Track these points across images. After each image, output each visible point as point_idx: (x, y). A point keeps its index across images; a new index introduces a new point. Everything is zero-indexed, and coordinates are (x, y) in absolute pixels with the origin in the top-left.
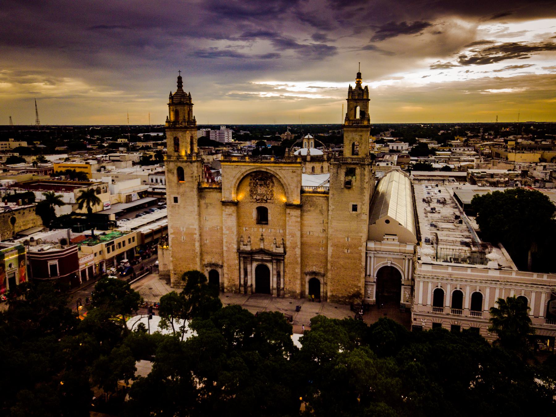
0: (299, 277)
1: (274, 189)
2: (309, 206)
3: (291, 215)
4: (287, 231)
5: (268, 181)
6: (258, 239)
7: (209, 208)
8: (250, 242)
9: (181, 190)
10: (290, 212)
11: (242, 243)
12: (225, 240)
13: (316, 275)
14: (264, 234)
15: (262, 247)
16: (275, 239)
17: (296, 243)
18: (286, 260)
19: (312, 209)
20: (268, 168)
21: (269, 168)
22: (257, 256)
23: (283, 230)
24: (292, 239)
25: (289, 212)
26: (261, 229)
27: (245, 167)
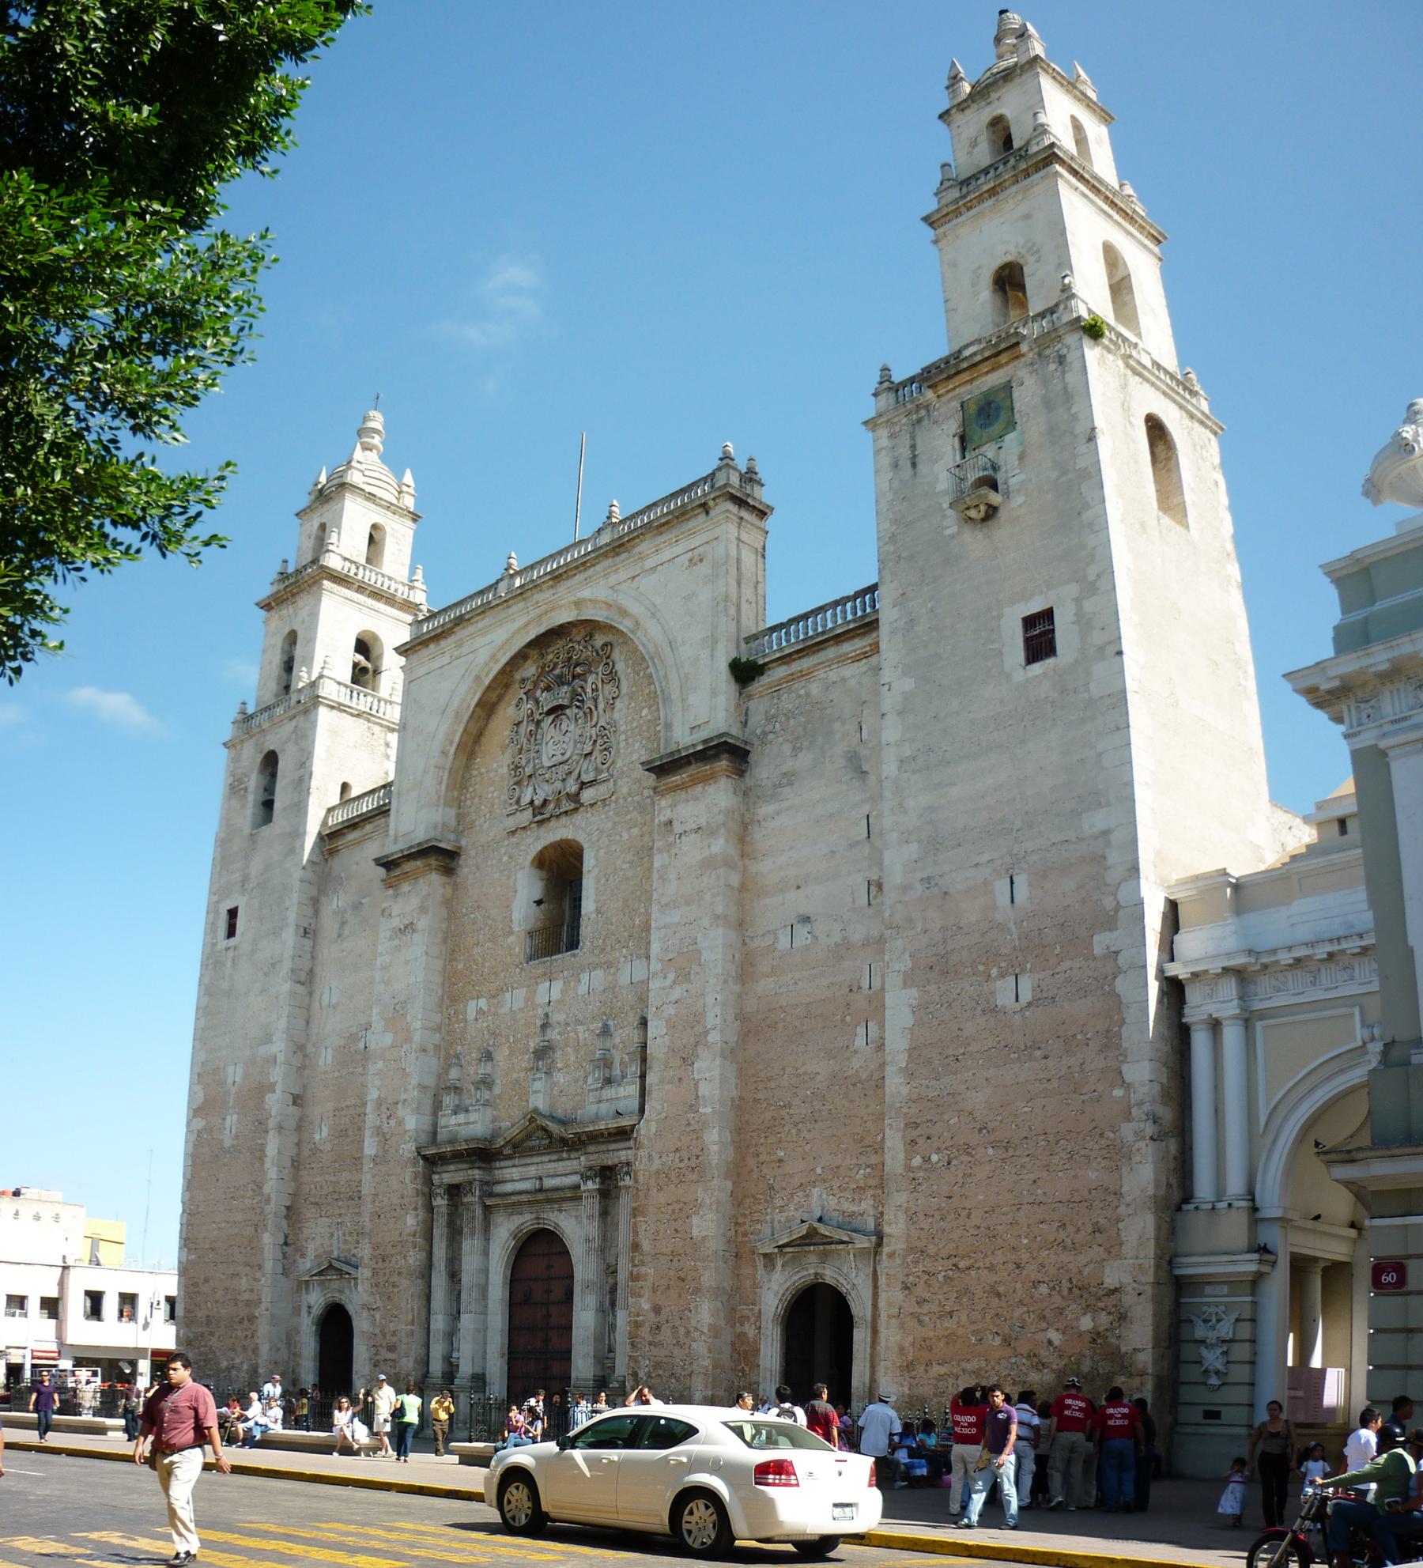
0: (709, 1278)
1: (616, 715)
2: (787, 749)
3: (678, 828)
4: (655, 948)
5: (591, 679)
7: (346, 932)
8: (486, 1083)
11: (449, 1100)
12: (373, 1094)
13: (824, 1258)
14: (555, 1018)
15: (539, 1102)
17: (698, 1017)
19: (805, 759)
21: (586, 593)
22: (514, 1173)
25: (665, 816)
27: (489, 638)
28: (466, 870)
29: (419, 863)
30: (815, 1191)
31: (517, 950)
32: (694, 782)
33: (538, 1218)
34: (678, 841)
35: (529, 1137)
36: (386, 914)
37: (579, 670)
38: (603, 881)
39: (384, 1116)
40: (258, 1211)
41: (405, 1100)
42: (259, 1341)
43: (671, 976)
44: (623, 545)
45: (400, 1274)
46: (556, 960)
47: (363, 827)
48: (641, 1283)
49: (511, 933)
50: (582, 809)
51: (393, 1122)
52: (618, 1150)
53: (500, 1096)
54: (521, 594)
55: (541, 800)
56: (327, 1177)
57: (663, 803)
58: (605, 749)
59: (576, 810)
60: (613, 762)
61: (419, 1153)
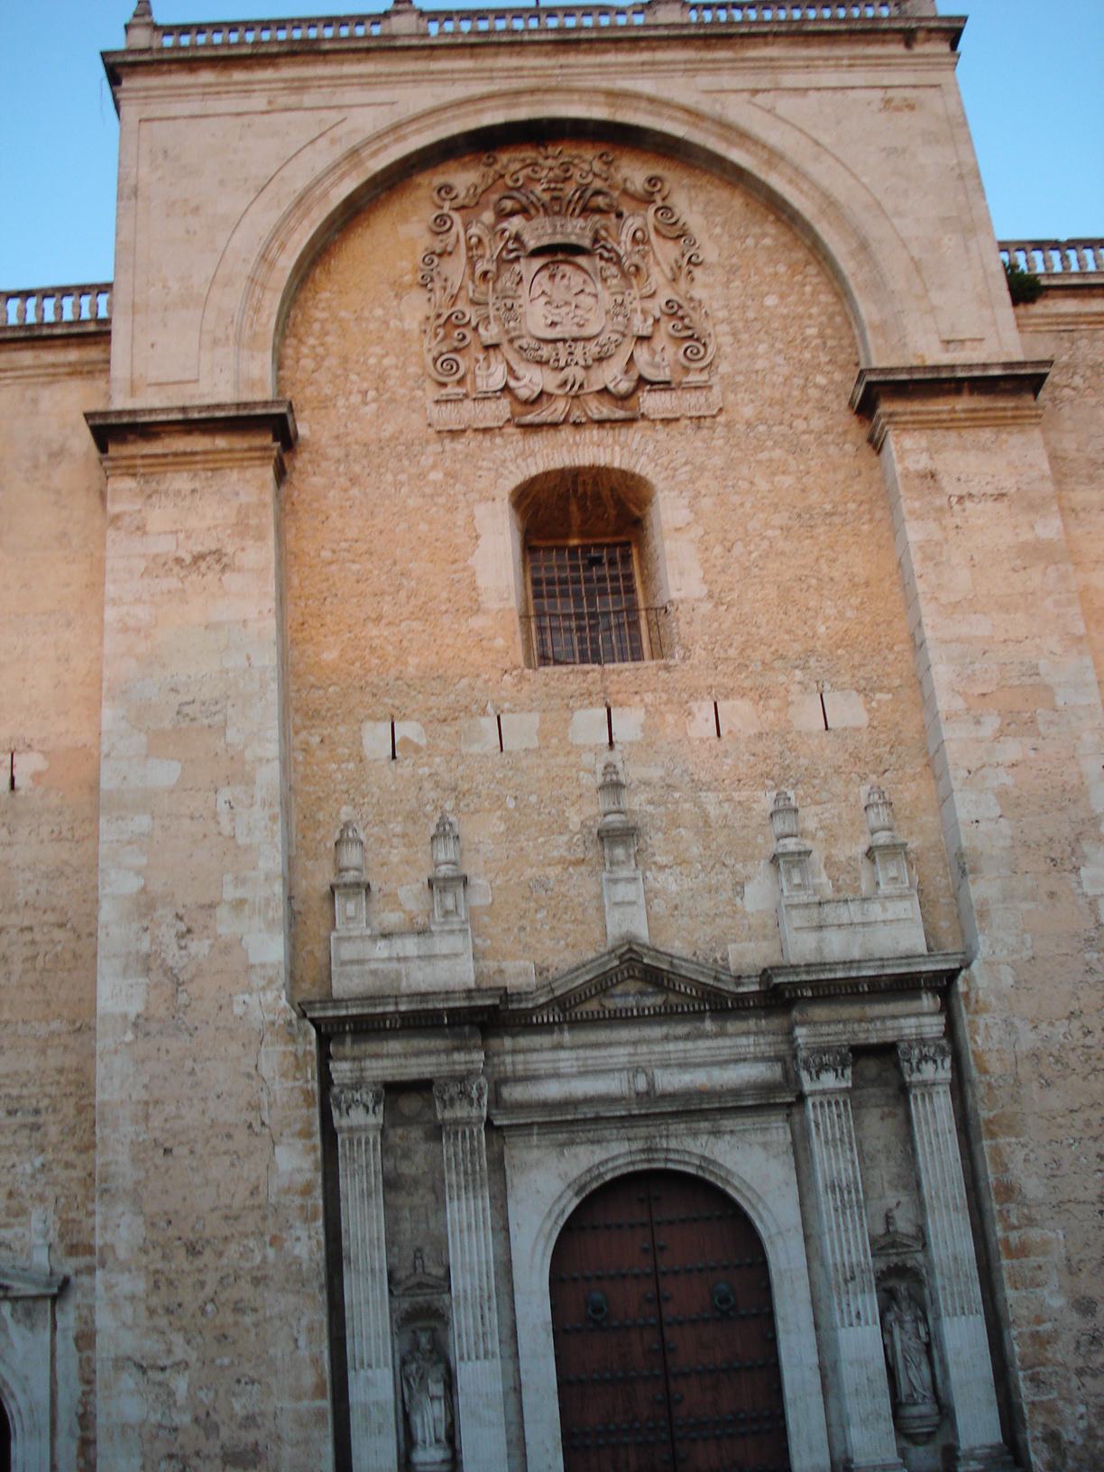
1: (698, 293)
4: (942, 674)
10: (938, 465)
12: (119, 884)
14: (631, 773)
16: (784, 809)
21: (645, 85)
22: (567, 1060)
23: (865, 692)
24: (1012, 749)
25: (922, 462)
27: (382, 95)
28: (317, 481)
29: (221, 442)
31: (500, 642)
32: (975, 420)
33: (643, 1151)
34: (957, 508)
36: (127, 519)
37: (600, 201)
38: (718, 550)
39: (168, 934)
41: (239, 904)
43: (991, 724)
45: (256, 1281)
46: (620, 673)
48: (1033, 1260)
49: (476, 609)
50: (641, 424)
51: (199, 947)
52: (894, 1017)
53: (489, 909)
55: (538, 391)
57: (908, 441)
58: (691, 337)
59: (630, 421)
60: (711, 364)
61: (303, 1015)
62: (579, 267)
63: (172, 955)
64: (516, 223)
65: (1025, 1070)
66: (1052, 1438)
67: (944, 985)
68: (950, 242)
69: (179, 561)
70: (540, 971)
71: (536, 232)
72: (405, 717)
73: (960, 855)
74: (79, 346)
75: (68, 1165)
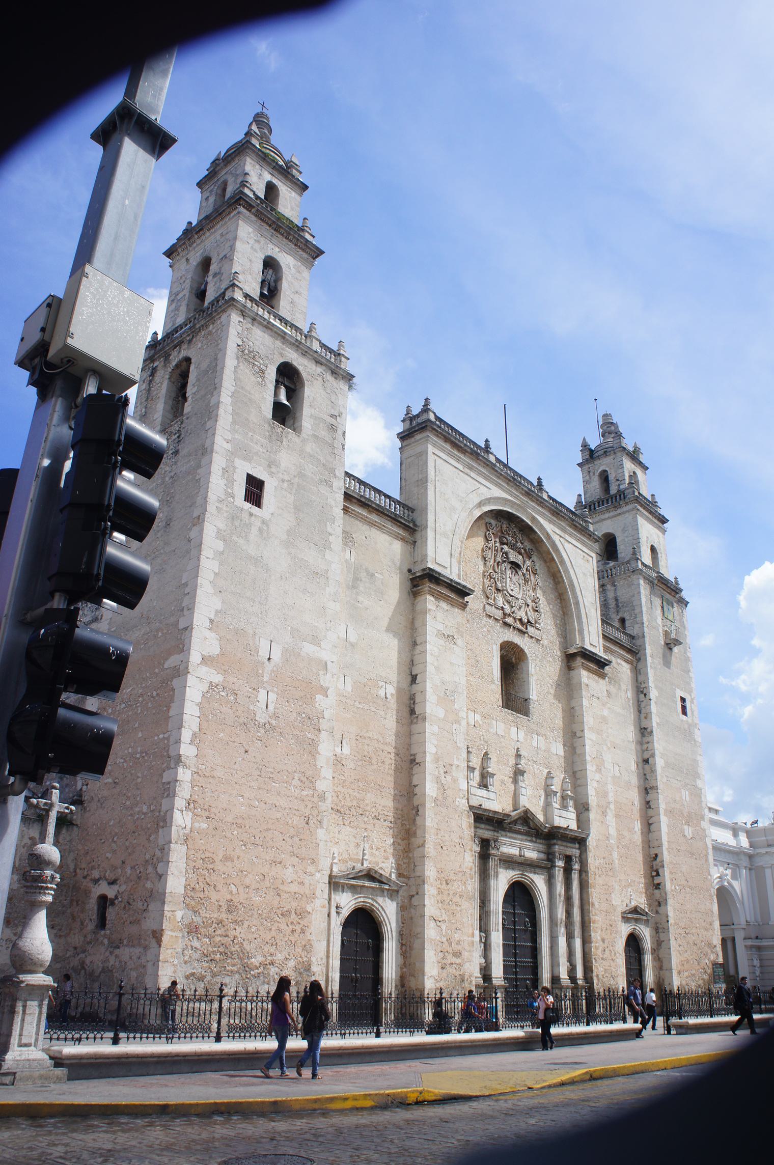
6: (508, 771)
7: (361, 588)
9: (287, 459)
13: (637, 920)
14: (522, 752)
17: (605, 795)
18: (593, 861)
20: (536, 516)
24: (597, 777)
26: (514, 729)
29: (453, 596)
30: (629, 890)
35: (515, 822)
36: (432, 613)
39: (442, 771)
40: (310, 805)
41: (458, 766)
42: (313, 937)
43: (594, 768)
44: (559, 514)
45: (461, 896)
47: (370, 512)
48: (596, 925)
51: (449, 778)
54: (510, 480)
56: (351, 791)
58: (537, 611)
59: (524, 633)
62: (517, 572)
63: (443, 780)
64: (506, 548)
65: (597, 871)
66: (597, 976)
67: (581, 842)
68: (593, 611)
69: (444, 635)
70: (503, 810)
71: (514, 557)
72: (477, 713)
73: (587, 804)
74: (403, 528)
75: (399, 844)
